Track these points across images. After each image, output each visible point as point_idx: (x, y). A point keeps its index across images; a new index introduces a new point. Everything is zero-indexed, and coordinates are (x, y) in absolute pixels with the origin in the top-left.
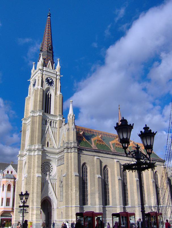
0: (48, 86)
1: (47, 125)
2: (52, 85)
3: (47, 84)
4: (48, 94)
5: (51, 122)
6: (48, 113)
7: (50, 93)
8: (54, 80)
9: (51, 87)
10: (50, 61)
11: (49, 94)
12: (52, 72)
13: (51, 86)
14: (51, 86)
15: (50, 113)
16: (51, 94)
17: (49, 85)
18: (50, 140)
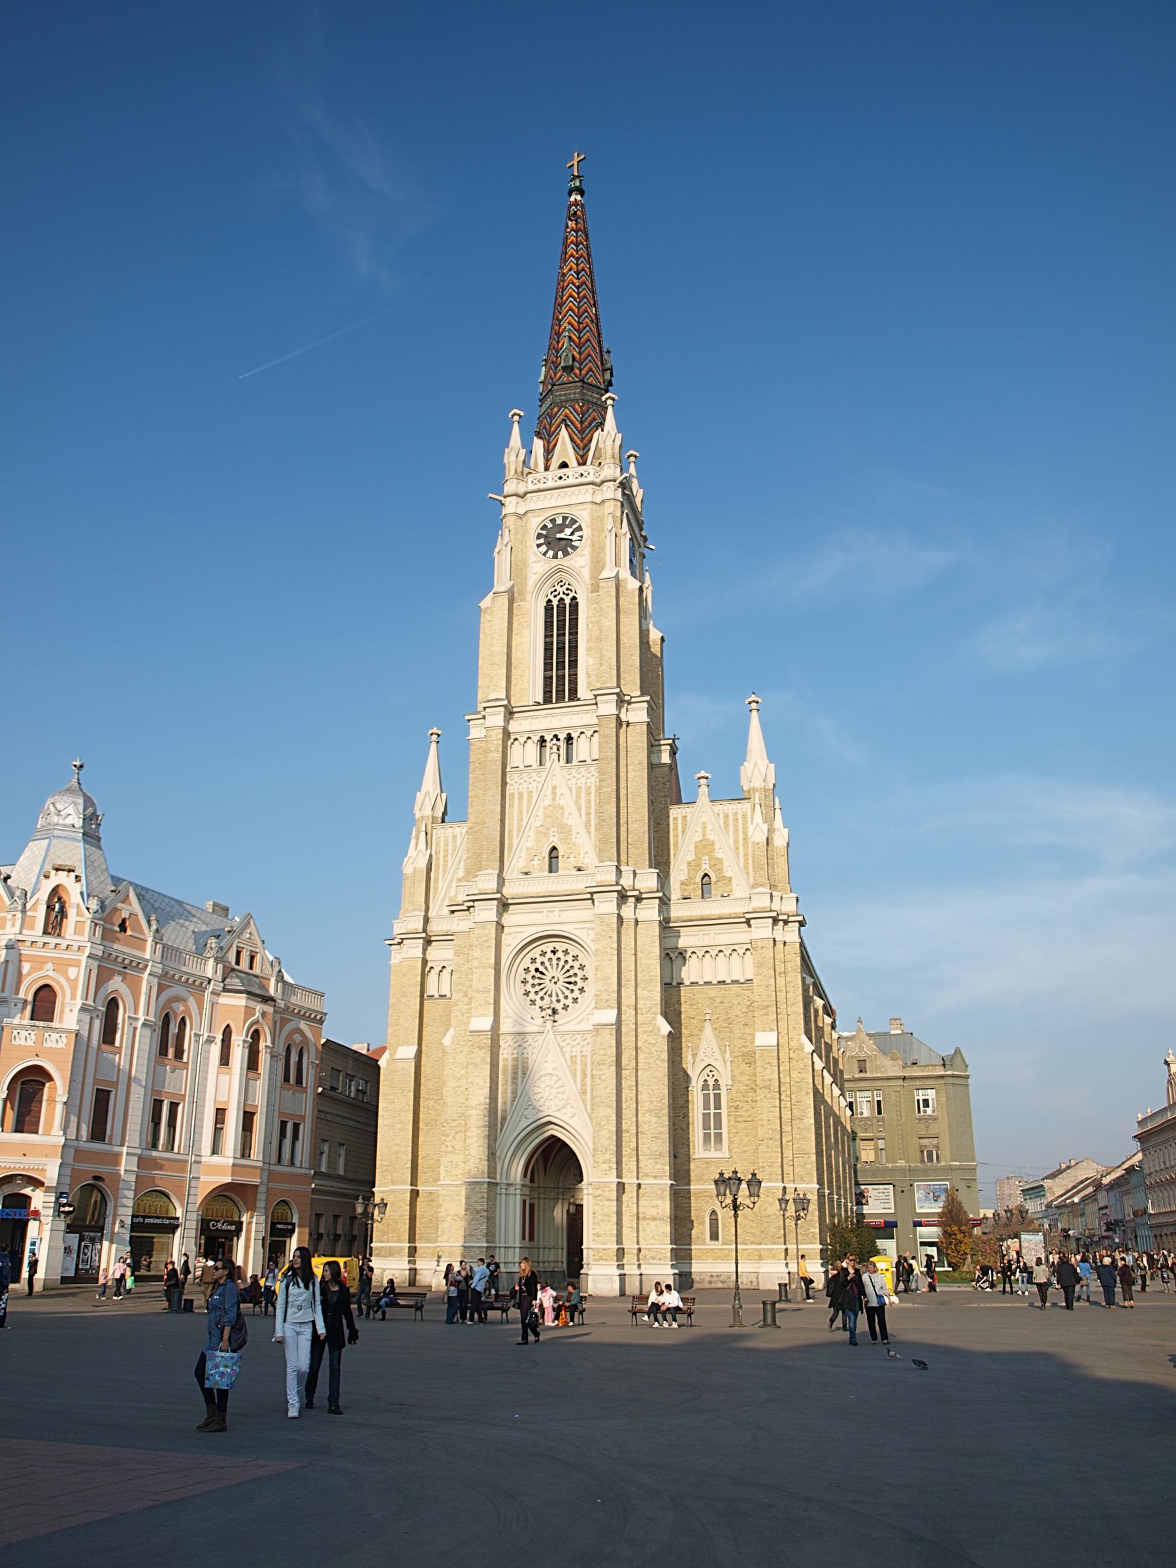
0: (556, 562)
1: (548, 764)
2: (574, 548)
3: (545, 554)
4: (562, 599)
5: (569, 738)
6: (560, 698)
7: (571, 595)
8: (584, 516)
9: (563, 561)
10: (564, 433)
11: (567, 601)
12: (571, 481)
13: (566, 554)
14: (566, 554)
15: (573, 695)
16: (574, 598)
17: (555, 557)
18: (566, 831)
